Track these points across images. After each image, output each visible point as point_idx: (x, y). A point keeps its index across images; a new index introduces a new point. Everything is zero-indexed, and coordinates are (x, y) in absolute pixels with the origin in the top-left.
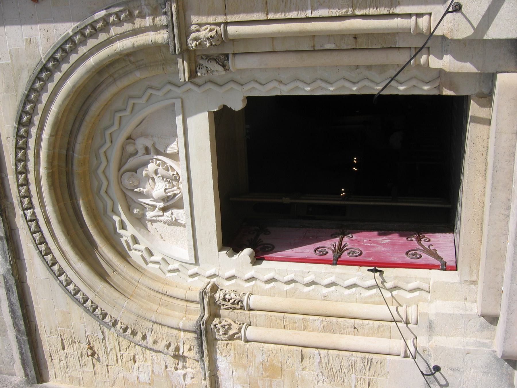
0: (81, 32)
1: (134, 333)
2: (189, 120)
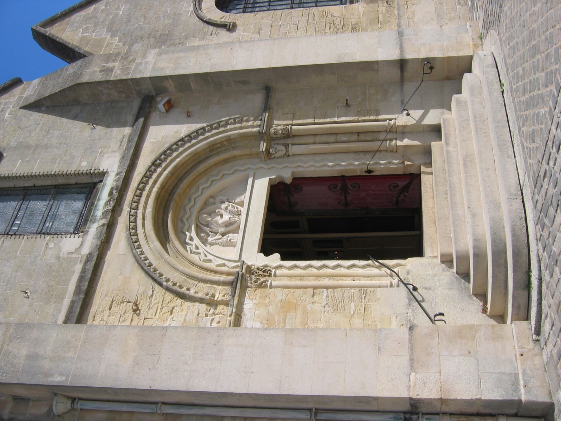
0: (211, 126)
1: (181, 287)
2: (256, 181)
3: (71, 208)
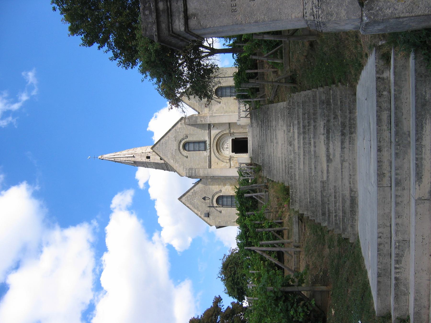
3: (202, 145)
